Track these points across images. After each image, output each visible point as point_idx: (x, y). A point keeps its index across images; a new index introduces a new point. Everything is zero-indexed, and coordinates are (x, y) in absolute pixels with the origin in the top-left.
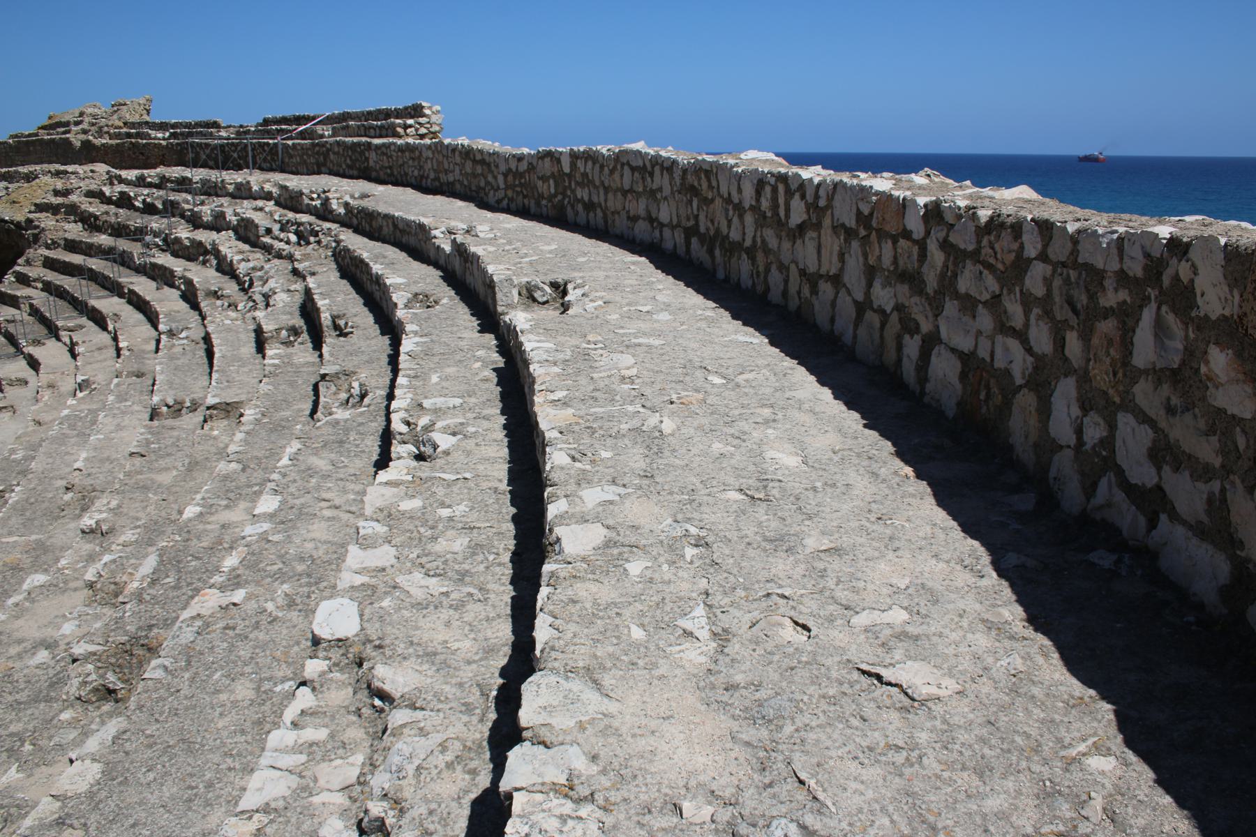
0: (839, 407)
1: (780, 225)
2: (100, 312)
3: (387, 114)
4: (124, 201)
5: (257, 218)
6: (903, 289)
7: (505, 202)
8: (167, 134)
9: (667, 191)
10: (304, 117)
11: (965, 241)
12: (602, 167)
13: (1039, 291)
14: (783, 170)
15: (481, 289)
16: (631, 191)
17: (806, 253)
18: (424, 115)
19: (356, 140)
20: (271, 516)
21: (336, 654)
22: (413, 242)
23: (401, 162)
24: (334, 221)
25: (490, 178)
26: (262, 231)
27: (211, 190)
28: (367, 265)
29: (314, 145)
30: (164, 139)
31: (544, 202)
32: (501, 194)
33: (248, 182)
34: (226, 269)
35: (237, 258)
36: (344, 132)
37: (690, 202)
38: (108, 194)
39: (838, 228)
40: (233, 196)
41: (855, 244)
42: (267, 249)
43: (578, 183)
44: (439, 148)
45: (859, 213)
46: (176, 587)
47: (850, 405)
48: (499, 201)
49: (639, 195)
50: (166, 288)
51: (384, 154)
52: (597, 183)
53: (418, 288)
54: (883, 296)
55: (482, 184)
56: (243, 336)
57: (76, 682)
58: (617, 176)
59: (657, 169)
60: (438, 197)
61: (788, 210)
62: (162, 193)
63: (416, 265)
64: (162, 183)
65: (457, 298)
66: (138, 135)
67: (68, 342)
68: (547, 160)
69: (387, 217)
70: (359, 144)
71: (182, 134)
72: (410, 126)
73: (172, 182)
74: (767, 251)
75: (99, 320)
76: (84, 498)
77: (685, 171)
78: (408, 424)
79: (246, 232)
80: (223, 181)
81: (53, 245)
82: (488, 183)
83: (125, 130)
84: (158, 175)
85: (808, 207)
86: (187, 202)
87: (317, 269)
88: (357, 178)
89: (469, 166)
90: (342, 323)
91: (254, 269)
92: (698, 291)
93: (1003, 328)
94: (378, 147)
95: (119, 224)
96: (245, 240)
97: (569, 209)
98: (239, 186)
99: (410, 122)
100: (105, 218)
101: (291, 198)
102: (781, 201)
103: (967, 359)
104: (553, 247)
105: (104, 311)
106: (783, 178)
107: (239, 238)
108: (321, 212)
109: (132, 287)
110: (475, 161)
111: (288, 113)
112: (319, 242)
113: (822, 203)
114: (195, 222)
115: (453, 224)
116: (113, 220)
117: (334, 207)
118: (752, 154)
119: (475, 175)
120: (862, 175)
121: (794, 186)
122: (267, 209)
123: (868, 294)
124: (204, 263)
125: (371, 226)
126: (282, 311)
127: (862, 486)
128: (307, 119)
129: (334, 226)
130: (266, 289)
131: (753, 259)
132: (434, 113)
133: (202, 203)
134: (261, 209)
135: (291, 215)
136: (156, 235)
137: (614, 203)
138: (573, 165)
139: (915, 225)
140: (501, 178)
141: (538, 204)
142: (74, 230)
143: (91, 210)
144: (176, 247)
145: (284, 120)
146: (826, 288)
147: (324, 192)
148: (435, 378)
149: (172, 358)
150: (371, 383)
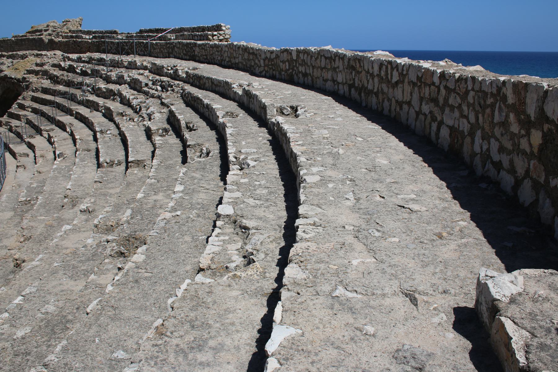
0: (406, 148)
1: (389, 82)
3: (203, 29)
5: (141, 78)
6: (432, 105)
8: (91, 37)
9: (341, 68)
10: (160, 29)
11: (451, 85)
13: (471, 101)
14: (390, 59)
15: (258, 110)
17: (398, 94)
18: (222, 30)
19: (188, 41)
20: (182, 192)
22: (223, 90)
23: (211, 52)
24: (180, 81)
26: (143, 85)
27: (116, 65)
28: (201, 100)
29: (166, 43)
30: (90, 39)
33: (135, 61)
34: (126, 102)
35: (131, 97)
36: (182, 38)
37: (352, 73)
38: (63, 66)
39: (411, 83)
40: (127, 68)
41: (416, 89)
42: (146, 93)
44: (231, 46)
45: (418, 76)
46: (142, 219)
47: (409, 148)
50: (95, 112)
51: (203, 48)
53: (228, 110)
54: (426, 108)
56: (139, 133)
57: (109, 249)
59: (337, 58)
60: (231, 70)
61: (392, 76)
62: (90, 65)
63: (224, 100)
64: (90, 61)
65: (246, 114)
69: (208, 78)
70: (190, 44)
71: (99, 37)
72: (215, 35)
73: (95, 60)
74: (383, 93)
77: (349, 59)
78: (236, 158)
79: (135, 85)
80: (122, 60)
81: (36, 90)
84: (87, 57)
85: (399, 74)
86: (104, 70)
87: (173, 102)
88: (189, 60)
89: (246, 55)
90: (191, 125)
91: (141, 102)
92: (354, 110)
93: (463, 116)
94: (200, 45)
95: (69, 80)
96: (135, 89)
98: (130, 63)
100: (62, 77)
101: (158, 69)
102: (389, 72)
103: (451, 128)
104: (290, 92)
106: (390, 62)
107: (131, 88)
108: (173, 76)
109: (77, 111)
110: (249, 53)
111: (153, 27)
112: (173, 90)
113: (405, 73)
114: (108, 80)
115: (241, 82)
116: (66, 78)
117: (180, 74)
118: (379, 52)
120: (421, 61)
121: (394, 66)
122: (145, 74)
123: (420, 108)
124: (114, 100)
125: (200, 83)
126: (159, 121)
128: (162, 31)
129: (180, 83)
130: (149, 111)
131: (377, 96)
133: (111, 71)
134: (142, 74)
135: (158, 77)
136: (88, 86)
137: (317, 73)
139: (436, 80)
142: (46, 83)
144: (99, 92)
145: (150, 31)
146: (405, 107)
147: (174, 66)
148: (244, 143)
149: (105, 142)
150: (211, 148)
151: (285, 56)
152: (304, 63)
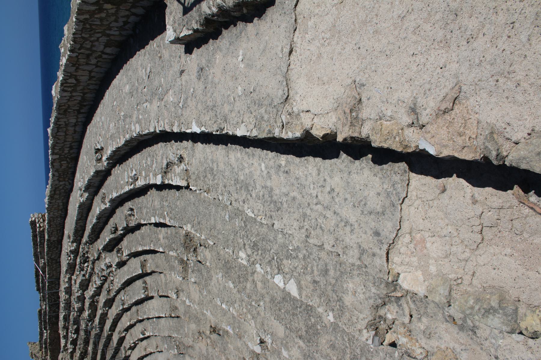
0: (119, 74)
1: (75, 86)
2: (119, 340)
3: (35, 236)
4: (74, 342)
5: (78, 281)
6: (91, 58)
7: (70, 181)
8: (45, 331)
9: (65, 120)
10: (36, 273)
12: (57, 143)
14: (59, 84)
15: (99, 178)
16: (65, 132)
17: (84, 79)
18: (35, 220)
19: (46, 246)
20: (155, 217)
21: (164, 178)
22: (85, 209)
23: (55, 226)
24: (79, 248)
25: (61, 188)
26: (84, 278)
27: (68, 304)
28: (94, 225)
29: (48, 265)
30: (47, 332)
31: (70, 166)
32: (67, 183)
33: (65, 288)
34: (98, 292)
35: (95, 286)
36: (43, 255)
37: (69, 112)
38: (71, 350)
39: (76, 71)
40: (70, 295)
41: (80, 67)
42: (91, 275)
43: (63, 152)
44: (49, 210)
45: (72, 66)
46: (174, 243)
47: (119, 72)
48: (70, 184)
49: (67, 130)
50: (108, 316)
51: (52, 234)
52: (63, 145)
53: (100, 201)
54: (93, 61)
55: (63, 191)
56: (121, 272)
57: (192, 258)
58: (60, 137)
59: (58, 123)
60: (69, 208)
61: (71, 83)
62: (70, 327)
63: (93, 207)
64: (66, 328)
65: (103, 187)
66: (46, 344)
67: (130, 351)
68: (54, 164)
69: (76, 223)
70: (48, 245)
71: (44, 325)
72: (40, 225)
73: (65, 324)
74: (84, 89)
75: (122, 340)
76: (173, 310)
77: (59, 114)
78: (131, 184)
79: (84, 286)
80: (64, 300)
82: (63, 189)
83: (43, 350)
84: (63, 331)
85: (70, 78)
86: (74, 314)
87: (97, 249)
88: (61, 245)
89: (57, 197)
90: (113, 229)
91: (98, 277)
92: (96, 109)
93: (98, 39)
94: (49, 237)
95: (84, 343)
96: (88, 285)
97: (72, 156)
98: (66, 293)
99: (38, 225)
100: (81, 349)
101: (70, 268)
102: (69, 85)
103: (106, 46)
104: (85, 157)
105: (118, 338)
106: (62, 84)
107: (87, 289)
108: (76, 254)
109: (108, 330)
110: (55, 194)
111: (34, 280)
112: (87, 252)
113: (69, 75)
114: (81, 310)
115: (78, 196)
116: (82, 345)
117: (73, 248)
118: (53, 92)
119: (60, 194)
120: (61, 63)
121: (64, 82)
122: (75, 278)
123: (93, 65)
124: (97, 302)
125: (80, 231)
126: (112, 259)
127: (130, 73)
128: (37, 272)
129: (81, 247)
130: (105, 268)
131: (86, 93)
132: (33, 217)
133: (74, 308)
134: (75, 281)
135: (77, 267)
136: (87, 325)
137: (70, 139)
138: (56, 154)
139: (75, 55)
140: (61, 183)
141: (70, 168)
143: (78, 355)
144: (92, 316)
145: (37, 282)
146: (93, 74)
147: (68, 255)
148: (122, 182)
149: (130, 298)
150: (128, 208)
151: (57, 164)
152: (62, 149)
